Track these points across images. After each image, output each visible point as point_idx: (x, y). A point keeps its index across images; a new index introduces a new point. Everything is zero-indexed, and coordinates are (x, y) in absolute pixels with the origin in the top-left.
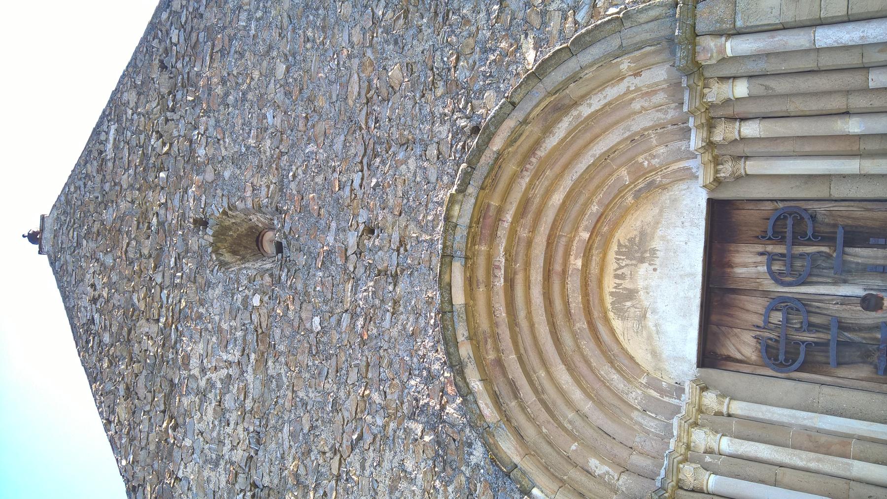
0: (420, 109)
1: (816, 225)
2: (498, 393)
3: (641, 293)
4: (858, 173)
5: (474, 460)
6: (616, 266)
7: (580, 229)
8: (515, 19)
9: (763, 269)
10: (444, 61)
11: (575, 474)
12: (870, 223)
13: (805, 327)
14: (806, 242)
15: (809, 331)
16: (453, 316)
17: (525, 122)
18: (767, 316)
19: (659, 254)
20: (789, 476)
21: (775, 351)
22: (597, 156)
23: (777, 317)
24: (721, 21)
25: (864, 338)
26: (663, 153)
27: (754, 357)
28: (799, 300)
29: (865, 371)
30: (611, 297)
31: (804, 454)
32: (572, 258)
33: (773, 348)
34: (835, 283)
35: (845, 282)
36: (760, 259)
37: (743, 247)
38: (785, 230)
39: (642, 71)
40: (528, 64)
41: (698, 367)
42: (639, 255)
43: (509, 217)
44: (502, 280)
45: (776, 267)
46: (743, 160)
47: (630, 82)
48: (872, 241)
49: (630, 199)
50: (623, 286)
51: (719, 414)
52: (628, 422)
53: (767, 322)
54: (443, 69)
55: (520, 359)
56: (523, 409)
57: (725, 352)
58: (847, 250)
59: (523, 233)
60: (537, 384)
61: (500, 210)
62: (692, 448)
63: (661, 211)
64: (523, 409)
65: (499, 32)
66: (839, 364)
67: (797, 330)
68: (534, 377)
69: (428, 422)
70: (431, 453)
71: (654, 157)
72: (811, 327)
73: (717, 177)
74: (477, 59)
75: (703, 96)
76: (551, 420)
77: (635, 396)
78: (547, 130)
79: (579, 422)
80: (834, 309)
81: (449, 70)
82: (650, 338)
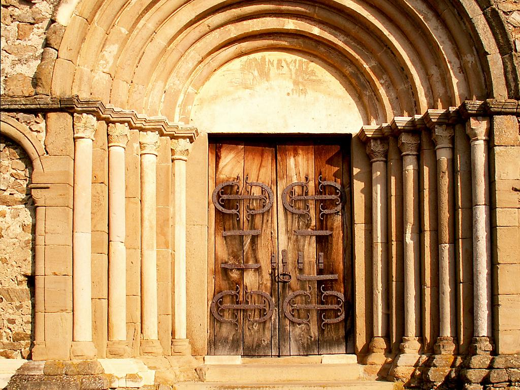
3: (266, 84)
4: (374, 241)
9: (295, 180)
13: (251, 212)
19: (302, 97)
21: (229, 191)
23: (256, 192)
27: (222, 176)
29: (223, 254)
30: (260, 58)
31: (154, 217)
33: (231, 191)
37: (312, 162)
38: (327, 194)
39: (463, 73)
41: (209, 134)
42: (301, 80)
45: (296, 188)
46: (384, 159)
52: (153, 78)
58: (314, 238)
63: (339, 97)
73: (370, 140)
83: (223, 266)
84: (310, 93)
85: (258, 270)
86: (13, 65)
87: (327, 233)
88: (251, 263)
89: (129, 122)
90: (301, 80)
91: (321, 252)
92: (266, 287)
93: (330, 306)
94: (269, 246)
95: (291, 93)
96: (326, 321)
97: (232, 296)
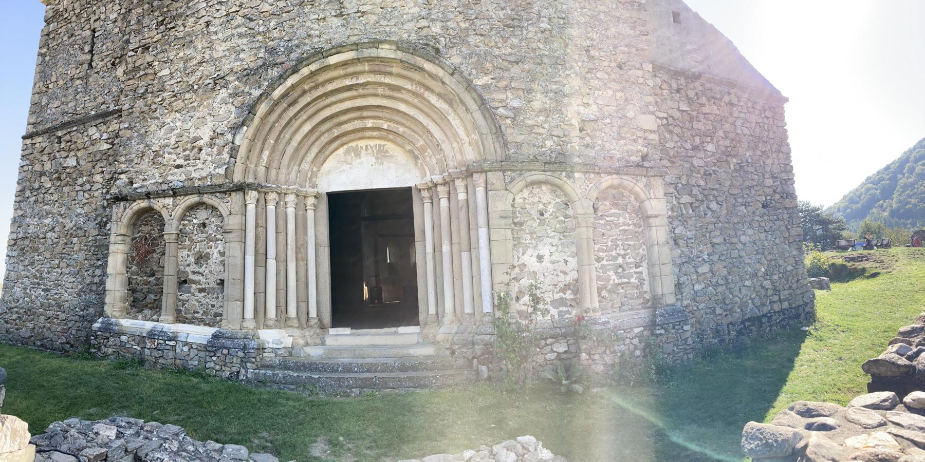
0: (451, 12)
3: (360, 161)
5: (253, 91)
6: (372, 145)
7: (388, 123)
11: (259, 145)
17: (443, 83)
32: (372, 121)
42: (380, 156)
43: (387, 80)
44: (350, 83)
47: (466, 140)
49: (408, 147)
52: (292, 164)
55: (308, 104)
59: (380, 91)
60: (300, 115)
61: (390, 74)
64: (284, 111)
68: (302, 113)
71: (430, 157)
75: (458, 178)
77: (305, 166)
78: (440, 95)
79: (285, 140)
81: (475, 30)
84: (386, 165)
86: (215, 169)
89: (276, 192)
95: (373, 164)
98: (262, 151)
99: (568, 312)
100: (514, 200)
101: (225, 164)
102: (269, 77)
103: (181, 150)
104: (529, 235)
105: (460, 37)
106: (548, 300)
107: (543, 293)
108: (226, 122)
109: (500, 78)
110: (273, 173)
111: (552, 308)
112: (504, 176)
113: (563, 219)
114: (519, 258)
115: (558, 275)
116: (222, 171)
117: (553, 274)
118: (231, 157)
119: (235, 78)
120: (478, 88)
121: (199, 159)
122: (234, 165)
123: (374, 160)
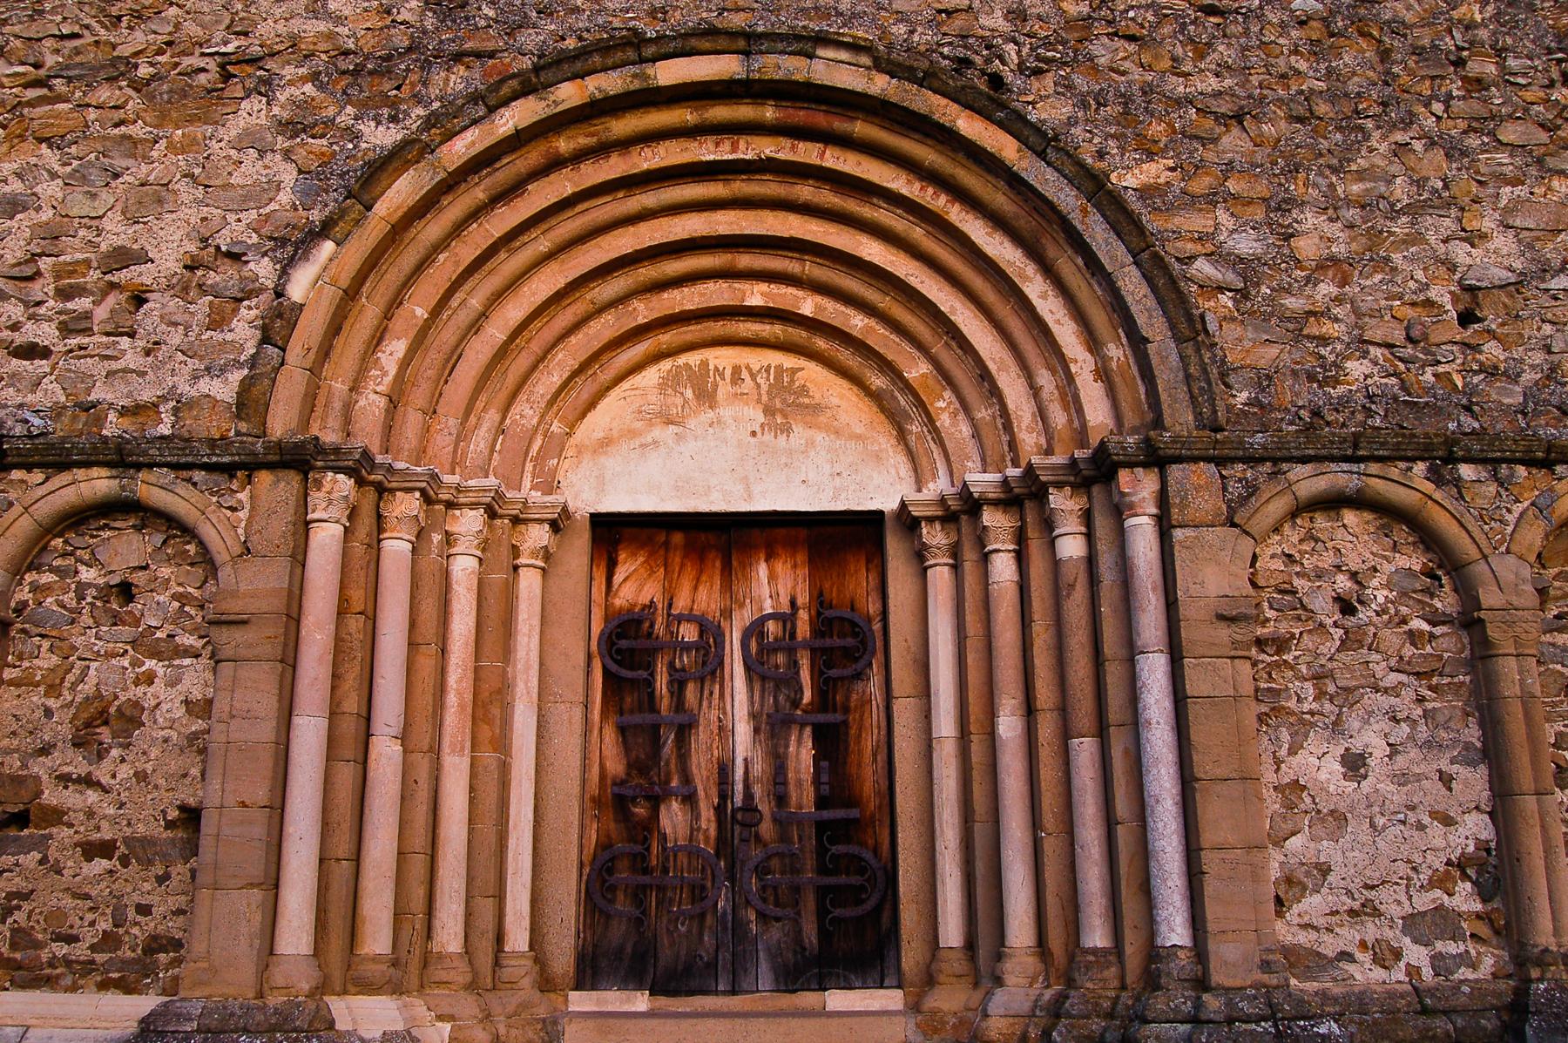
1: (846, 682)
2: (497, 165)
3: (711, 414)
6: (755, 367)
7: (818, 299)
8: (1203, 145)
10: (1127, 11)
12: (853, 758)
13: (677, 675)
14: (817, 668)
15: (670, 683)
16: (633, 63)
18: (690, 618)
19: (782, 439)
20: (427, 663)
21: (632, 633)
22: (952, 318)
23: (689, 633)
24: (1183, 506)
25: (667, 763)
26: (961, 431)
27: (618, 602)
28: (721, 664)
29: (616, 767)
31: (468, 684)
32: (764, 287)
34: (753, 716)
35: (756, 731)
36: (785, 601)
37: (803, 572)
40: (1119, 177)
42: (778, 405)
45: (771, 626)
46: (951, 561)
48: (825, 764)
50: (721, 383)
51: (515, 551)
52: (480, 404)
53: (680, 619)
54: (1112, 11)
56: (475, 215)
57: (622, 556)
58: (808, 731)
60: (525, 238)
62: (450, 512)
63: (859, 437)
64: (475, 215)
65: (1180, 117)
66: (622, 730)
67: (671, 665)
69: (425, 32)
70: (369, 46)
72: (678, 684)
74: (1131, 77)
75: (1059, 485)
76: (461, 269)
77: (526, 413)
79: (463, 318)
80: (709, 716)
81: (1110, 23)
82: (632, 434)
83: (616, 789)
84: (798, 429)
85: (690, 799)
86: (195, 378)
87: (838, 717)
88: (674, 783)
90: (778, 405)
91: (825, 759)
92: (707, 838)
93: (843, 879)
94: (715, 746)
95: (758, 430)
96: (838, 912)
97: (635, 856)
98: (378, 339)
99: (1464, 959)
100: (1255, 557)
101: (238, 365)
102: (434, 91)
103: (50, 290)
104: (1308, 685)
105: (1064, 43)
106: (1395, 911)
107: (1373, 887)
108: (253, 214)
109: (1197, 167)
110: (411, 421)
111: (1407, 940)
112: (1223, 477)
113: (1425, 627)
114: (1278, 763)
115: (1421, 827)
116: (224, 389)
117: (1403, 822)
118: (266, 340)
119: (303, 71)
120: (1131, 198)
121: (132, 335)
122: (277, 370)
123: (760, 417)
